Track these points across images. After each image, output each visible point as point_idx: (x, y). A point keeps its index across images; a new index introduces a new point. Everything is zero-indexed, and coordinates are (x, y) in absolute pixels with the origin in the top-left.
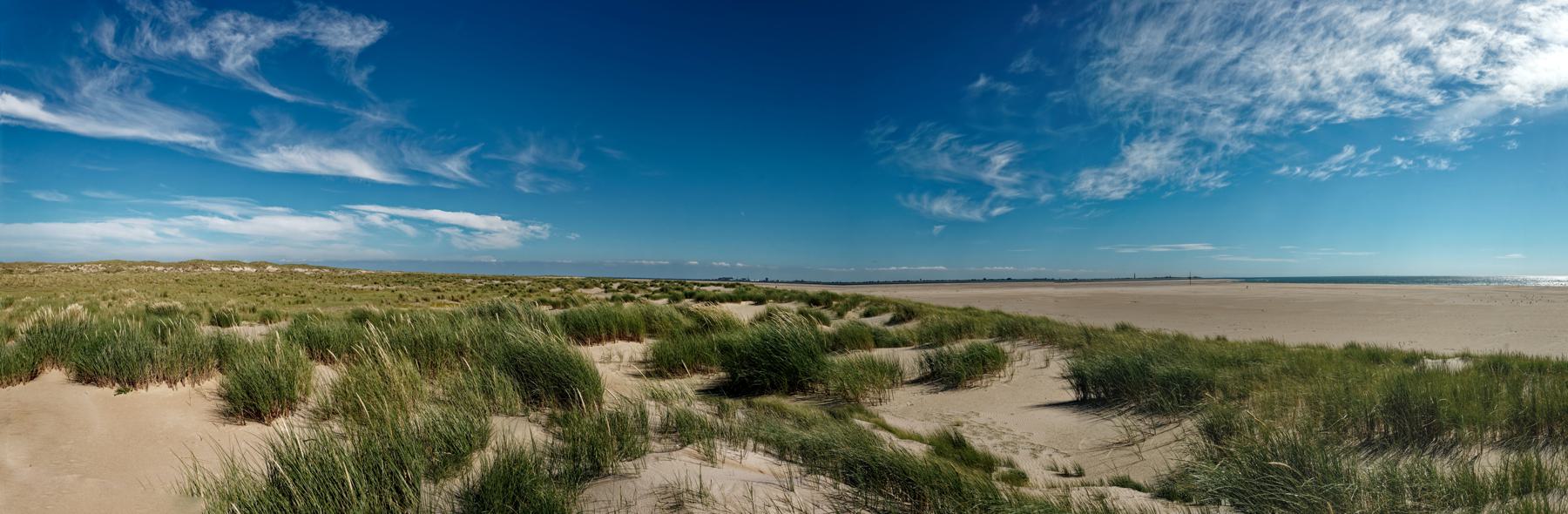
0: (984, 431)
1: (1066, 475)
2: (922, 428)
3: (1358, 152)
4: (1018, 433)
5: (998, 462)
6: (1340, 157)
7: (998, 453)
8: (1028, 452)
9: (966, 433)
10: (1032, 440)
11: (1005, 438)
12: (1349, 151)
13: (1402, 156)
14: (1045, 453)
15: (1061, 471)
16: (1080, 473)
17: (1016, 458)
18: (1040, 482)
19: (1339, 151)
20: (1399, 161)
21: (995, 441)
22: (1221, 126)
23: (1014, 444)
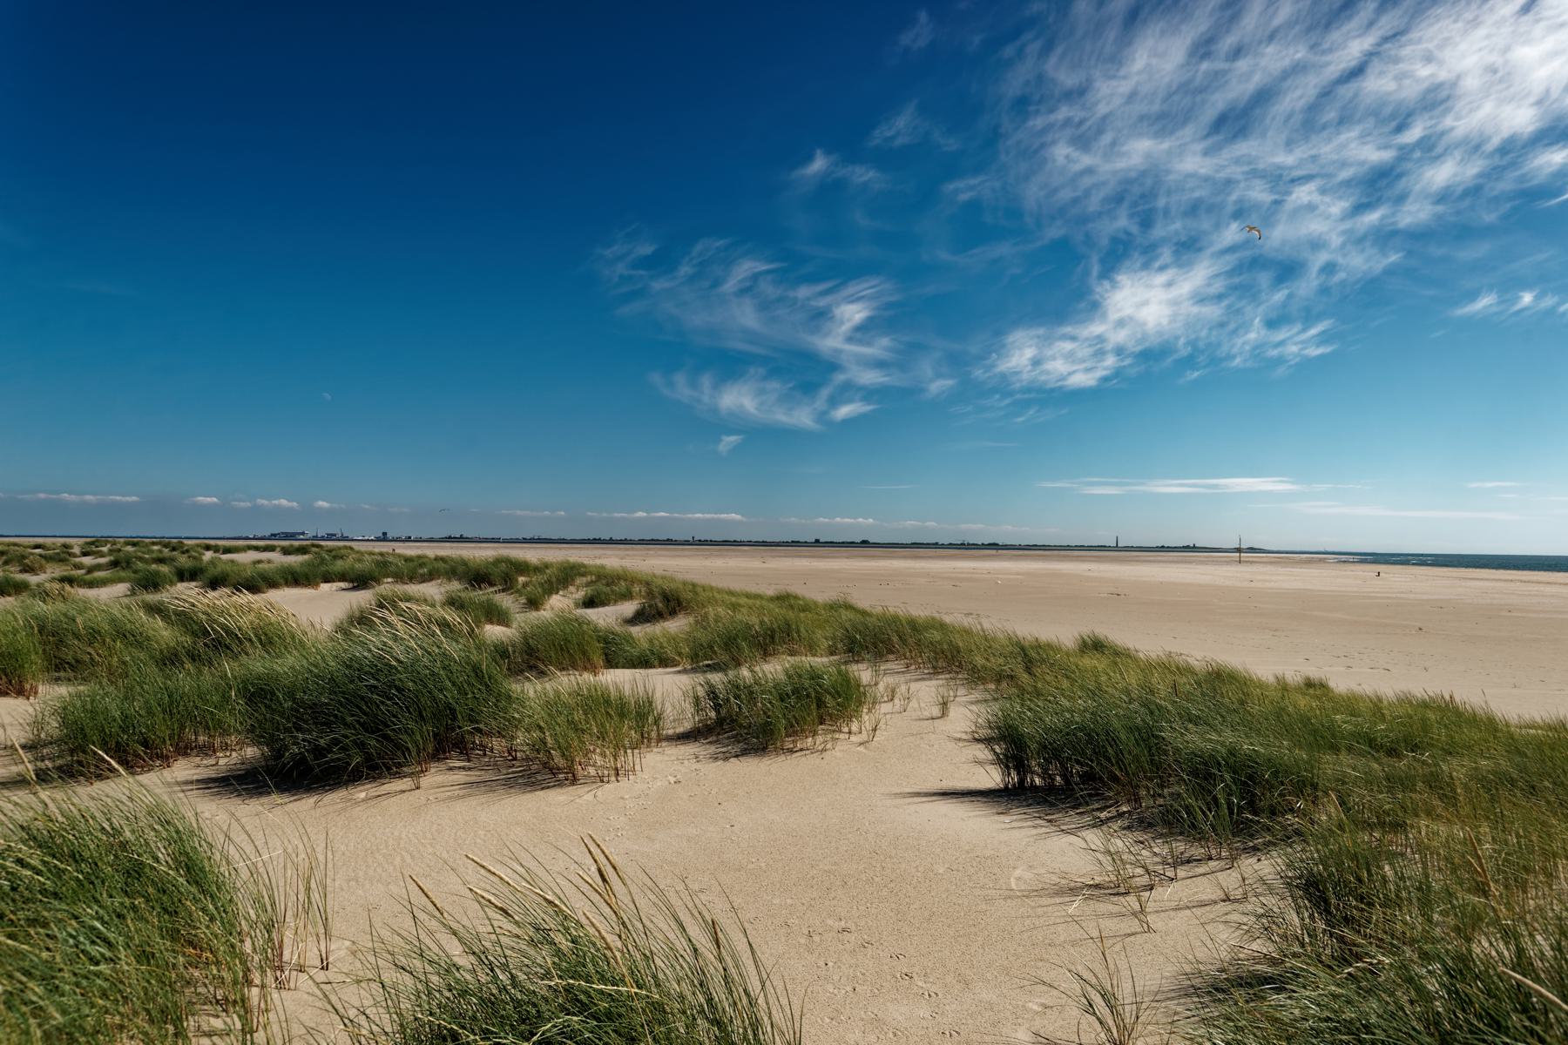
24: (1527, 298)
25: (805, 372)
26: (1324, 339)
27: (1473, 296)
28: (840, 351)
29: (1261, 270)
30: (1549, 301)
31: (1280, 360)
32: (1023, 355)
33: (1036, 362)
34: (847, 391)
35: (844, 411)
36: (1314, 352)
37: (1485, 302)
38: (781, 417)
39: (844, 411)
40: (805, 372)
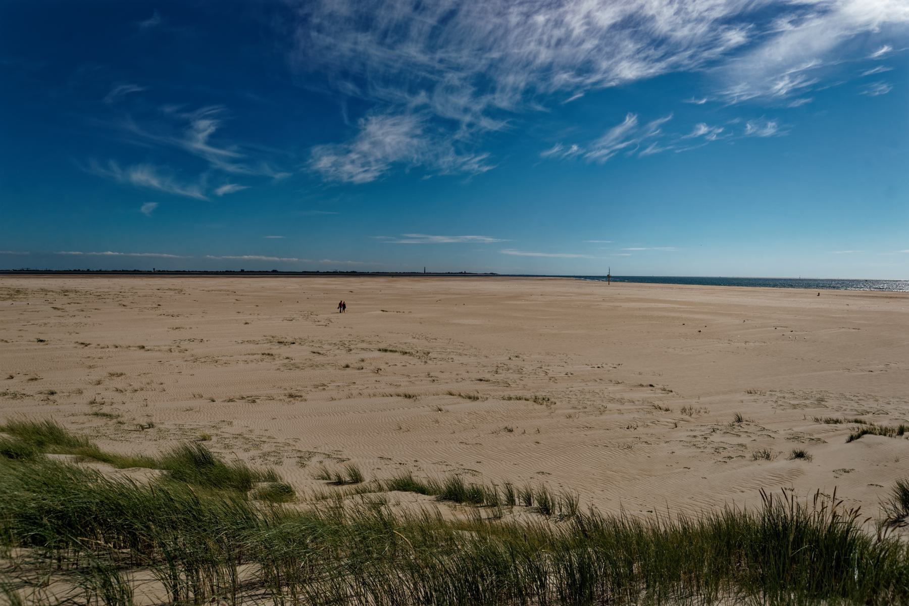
0: (239, 442)
1: (340, 482)
2: (152, 449)
3: (642, 123)
4: (281, 440)
5: (257, 477)
6: (618, 131)
7: (257, 466)
8: (294, 461)
9: (214, 448)
10: (298, 446)
11: (266, 448)
12: (630, 121)
13: (709, 124)
14: (315, 460)
15: (334, 479)
16: (356, 478)
17: (278, 470)
18: (309, 494)
19: (621, 120)
20: (703, 129)
21: (253, 452)
22: (458, 103)
23: (277, 453)
24: (575, 148)
25: (190, 166)
26: (488, 162)
27: (550, 146)
28: (203, 152)
29: (438, 126)
30: (581, 152)
31: (467, 174)
32: (324, 161)
33: (334, 164)
34: (219, 177)
35: (226, 189)
36: (485, 169)
37: (556, 149)
38: (177, 190)
39: (226, 189)
40: (190, 166)
